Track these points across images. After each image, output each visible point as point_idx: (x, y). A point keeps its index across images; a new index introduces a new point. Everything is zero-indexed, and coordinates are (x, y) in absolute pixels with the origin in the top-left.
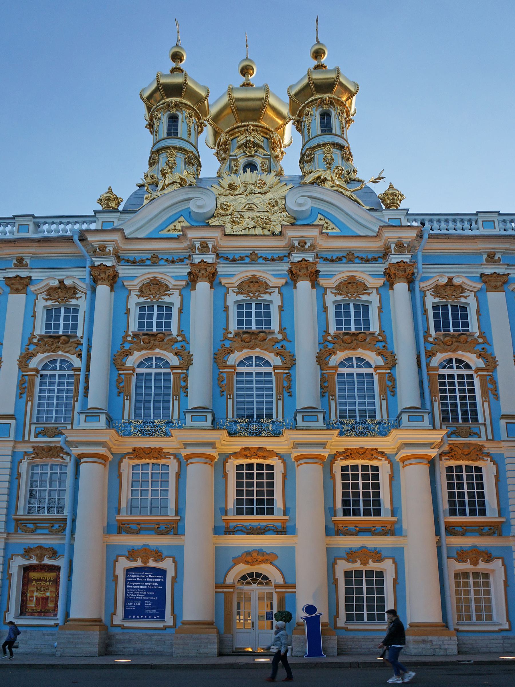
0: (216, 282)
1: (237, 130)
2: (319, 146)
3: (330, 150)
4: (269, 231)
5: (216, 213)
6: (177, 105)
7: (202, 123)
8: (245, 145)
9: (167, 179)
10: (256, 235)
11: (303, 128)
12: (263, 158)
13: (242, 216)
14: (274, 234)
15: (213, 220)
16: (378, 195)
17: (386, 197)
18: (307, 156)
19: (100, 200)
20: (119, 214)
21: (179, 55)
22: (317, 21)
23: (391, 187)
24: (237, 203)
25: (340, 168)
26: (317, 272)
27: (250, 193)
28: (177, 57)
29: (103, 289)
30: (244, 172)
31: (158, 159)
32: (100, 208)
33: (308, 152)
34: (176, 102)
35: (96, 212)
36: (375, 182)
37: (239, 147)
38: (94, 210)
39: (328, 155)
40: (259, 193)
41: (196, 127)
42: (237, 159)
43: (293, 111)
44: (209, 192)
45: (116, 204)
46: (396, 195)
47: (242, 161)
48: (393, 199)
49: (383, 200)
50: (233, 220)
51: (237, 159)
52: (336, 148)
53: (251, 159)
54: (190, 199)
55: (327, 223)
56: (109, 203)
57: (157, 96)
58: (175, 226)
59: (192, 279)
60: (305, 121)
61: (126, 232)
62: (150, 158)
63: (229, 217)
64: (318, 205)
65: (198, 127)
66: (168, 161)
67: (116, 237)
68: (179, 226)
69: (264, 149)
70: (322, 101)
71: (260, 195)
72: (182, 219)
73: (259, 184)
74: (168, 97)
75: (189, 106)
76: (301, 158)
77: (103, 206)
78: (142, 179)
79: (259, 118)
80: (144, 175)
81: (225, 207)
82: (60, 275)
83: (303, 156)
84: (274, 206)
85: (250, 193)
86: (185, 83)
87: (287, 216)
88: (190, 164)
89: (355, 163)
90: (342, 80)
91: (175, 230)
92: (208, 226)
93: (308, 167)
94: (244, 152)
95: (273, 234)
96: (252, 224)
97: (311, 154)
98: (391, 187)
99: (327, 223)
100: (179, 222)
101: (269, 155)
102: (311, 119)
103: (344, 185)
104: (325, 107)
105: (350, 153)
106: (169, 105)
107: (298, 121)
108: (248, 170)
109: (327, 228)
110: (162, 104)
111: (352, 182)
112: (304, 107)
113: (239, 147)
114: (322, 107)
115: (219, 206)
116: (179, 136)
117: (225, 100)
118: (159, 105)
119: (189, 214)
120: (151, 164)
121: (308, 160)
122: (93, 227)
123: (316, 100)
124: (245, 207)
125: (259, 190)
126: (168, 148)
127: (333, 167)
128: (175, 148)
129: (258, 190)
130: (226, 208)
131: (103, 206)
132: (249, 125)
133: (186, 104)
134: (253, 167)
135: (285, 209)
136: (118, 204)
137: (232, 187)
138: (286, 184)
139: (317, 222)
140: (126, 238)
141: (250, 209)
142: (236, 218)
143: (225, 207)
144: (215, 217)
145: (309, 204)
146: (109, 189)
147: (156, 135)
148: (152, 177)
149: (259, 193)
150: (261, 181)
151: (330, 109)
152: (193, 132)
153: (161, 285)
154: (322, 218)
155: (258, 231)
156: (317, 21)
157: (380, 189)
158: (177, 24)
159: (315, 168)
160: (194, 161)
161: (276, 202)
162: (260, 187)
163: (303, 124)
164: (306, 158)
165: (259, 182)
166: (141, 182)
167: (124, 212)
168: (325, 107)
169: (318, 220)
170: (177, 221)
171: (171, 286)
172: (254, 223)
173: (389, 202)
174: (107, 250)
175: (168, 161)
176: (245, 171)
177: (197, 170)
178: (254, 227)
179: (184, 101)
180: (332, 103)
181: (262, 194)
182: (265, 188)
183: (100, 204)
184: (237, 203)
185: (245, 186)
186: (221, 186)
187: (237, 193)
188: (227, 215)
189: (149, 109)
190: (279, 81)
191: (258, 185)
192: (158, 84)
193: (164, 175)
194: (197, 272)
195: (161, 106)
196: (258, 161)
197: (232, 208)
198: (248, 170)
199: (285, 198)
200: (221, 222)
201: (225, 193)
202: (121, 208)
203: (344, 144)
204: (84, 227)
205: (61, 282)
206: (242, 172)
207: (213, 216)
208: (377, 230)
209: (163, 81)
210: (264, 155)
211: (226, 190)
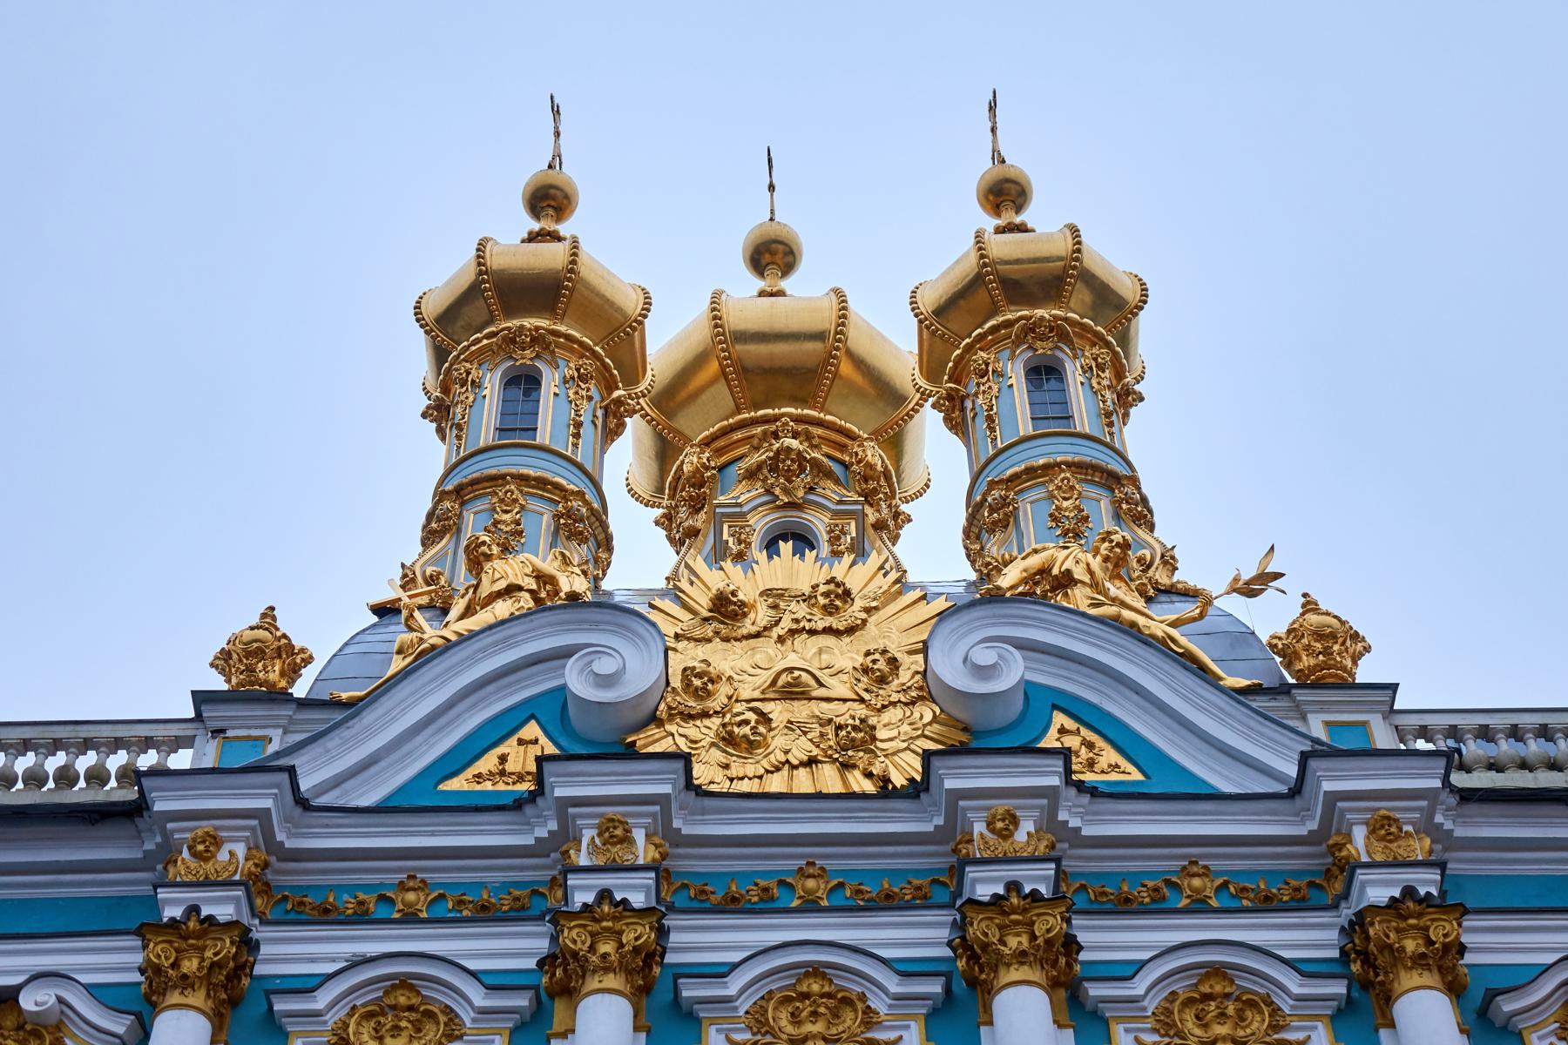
0: (662, 994)
1: (738, 435)
2: (1031, 472)
3: (1072, 488)
4: (869, 775)
5: (662, 706)
6: (539, 340)
7: (619, 402)
8: (774, 465)
9: (485, 579)
10: (819, 796)
11: (970, 415)
12: (836, 514)
13: (764, 718)
14: (886, 790)
15: (653, 731)
16: (1265, 639)
17: (1299, 646)
18: (992, 510)
19: (225, 655)
20: (287, 711)
21: (554, 198)
22: (992, 108)
23: (1310, 606)
24: (743, 667)
25: (1117, 538)
26: (1071, 945)
27: (793, 632)
28: (548, 200)
30: (770, 557)
31: (460, 516)
32: (218, 683)
33: (996, 493)
34: (537, 329)
35: (201, 698)
36: (1250, 589)
37: (751, 475)
38: (194, 693)
39: (1065, 504)
40: (828, 631)
41: (600, 413)
42: (743, 515)
43: (931, 366)
44: (640, 627)
45: (282, 674)
46: (1333, 636)
47: (760, 523)
48: (1327, 652)
49: (1289, 657)
50: (731, 733)
51: (743, 515)
52: (1092, 482)
53: (793, 516)
54: (565, 653)
55: (1090, 746)
56: (256, 671)
57: (476, 311)
58: (503, 759)
59: (562, 979)
60: (976, 395)
61: (305, 785)
62: (430, 516)
63: (716, 722)
64: (1049, 677)
65: (606, 415)
66: (496, 523)
67: (262, 798)
68: (520, 759)
69: (837, 482)
71: (829, 641)
72: (532, 730)
73: (826, 595)
74: (510, 313)
75: (581, 344)
76: (972, 518)
77: (234, 680)
78: (391, 581)
79: (815, 396)
80: (400, 572)
81: (697, 682)
83: (974, 510)
84: (882, 680)
85: (792, 632)
86: (571, 271)
87: (935, 719)
88: (578, 537)
89: (1167, 530)
90: (1088, 261)
91: (502, 773)
92: (630, 753)
93: (994, 548)
94: (768, 492)
95: (884, 787)
96: (801, 748)
97: (1004, 502)
98: (1310, 606)
99: (1090, 746)
100: (521, 742)
101: (856, 502)
102: (995, 388)
103: (1140, 603)
104: (1043, 348)
105: (1144, 500)
106: (511, 341)
107: (950, 397)
108: (786, 547)
109: (1091, 764)
110: (488, 337)
111: (1163, 598)
112: (969, 349)
113: (751, 475)
114: (1030, 347)
115: (676, 682)
116: (543, 437)
117: (701, 335)
118: (479, 340)
119: (556, 709)
120: (430, 537)
121: (995, 523)
122: (181, 760)
123: (1008, 324)
124: (774, 683)
125: (830, 621)
126: (497, 479)
127: (1093, 537)
128: (523, 479)
130: (704, 688)
131: (234, 680)
132: (783, 415)
133: (568, 337)
134: (803, 541)
136: (293, 673)
137: (726, 609)
138: (924, 597)
139: (1050, 741)
140: (302, 802)
142: (739, 724)
143: (700, 683)
144: (660, 723)
145: (1014, 671)
146: (264, 616)
147: (459, 437)
148: (431, 580)
149: (828, 631)
150: (832, 586)
151: (1060, 355)
152: (587, 431)
153: (430, 1015)
154: (1070, 724)
155: (829, 779)
156: (992, 108)
157: (1269, 617)
158: (556, 111)
159: (1021, 549)
160: (587, 528)
161: (893, 662)
162: (829, 610)
163: (968, 404)
164: (988, 517)
165: (822, 589)
166: (388, 592)
167: (303, 704)
168: (1043, 348)
169: (1053, 732)
170: (513, 741)
172: (810, 746)
173: (1312, 662)
174: (223, 856)
175: (496, 523)
176: (771, 547)
177: (596, 560)
178: (811, 762)
179: (562, 328)
180: (1064, 337)
181: (836, 633)
182: (855, 611)
183: (222, 672)
184: (743, 667)
185: (775, 607)
186: (685, 606)
187: (745, 631)
188: (705, 715)
189: (440, 355)
190: (880, 280)
191: (822, 601)
192: (481, 273)
193: (477, 561)
194: (582, 947)
195: (485, 342)
196: (819, 523)
197: (723, 690)
198: (786, 547)
199: (924, 649)
200: (682, 742)
201: (697, 633)
202: (300, 690)
203: (1116, 466)
204: (148, 760)
206: (762, 556)
207: (654, 719)
208: (1293, 771)
209: (496, 261)
210: (840, 502)
211: (706, 619)
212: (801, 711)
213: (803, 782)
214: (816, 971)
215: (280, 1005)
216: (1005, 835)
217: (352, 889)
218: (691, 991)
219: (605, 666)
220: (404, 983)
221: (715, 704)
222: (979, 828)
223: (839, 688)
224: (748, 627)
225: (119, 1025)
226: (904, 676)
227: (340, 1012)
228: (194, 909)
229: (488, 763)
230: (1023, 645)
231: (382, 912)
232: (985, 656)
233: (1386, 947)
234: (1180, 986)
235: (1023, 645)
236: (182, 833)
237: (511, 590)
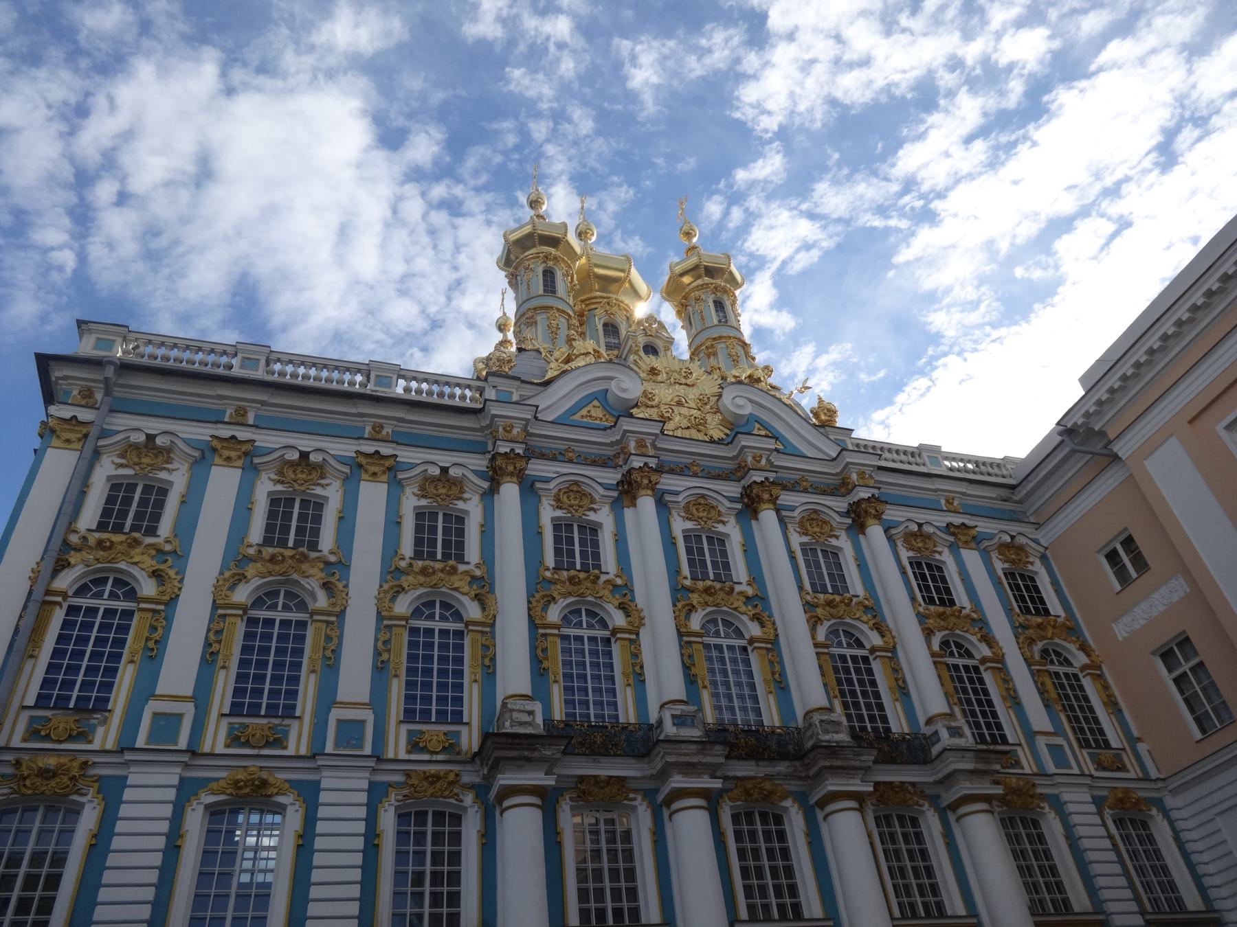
14: (712, 441)
29: (510, 492)
44: (632, 373)
54: (611, 378)
63: (655, 410)
70: (716, 288)
82: (445, 459)
96: (685, 423)
128: (558, 310)
129: (683, 381)
135: (718, 411)
141: (679, 404)
171: (597, 497)
205: (445, 470)
207: (636, 405)
212: (684, 411)
213: (687, 434)
214: (703, 496)
215: (538, 485)
216: (759, 462)
217: (551, 449)
218: (668, 498)
219: (624, 386)
220: (576, 483)
221: (654, 403)
222: (750, 459)
223: (692, 405)
224: (659, 378)
225: (486, 485)
226: (711, 403)
227: (555, 491)
228: (512, 450)
229: (584, 412)
230: (751, 401)
231: (561, 458)
232: (740, 401)
233: (866, 512)
234: (805, 514)
235: (751, 401)
236: (499, 421)
237: (587, 354)
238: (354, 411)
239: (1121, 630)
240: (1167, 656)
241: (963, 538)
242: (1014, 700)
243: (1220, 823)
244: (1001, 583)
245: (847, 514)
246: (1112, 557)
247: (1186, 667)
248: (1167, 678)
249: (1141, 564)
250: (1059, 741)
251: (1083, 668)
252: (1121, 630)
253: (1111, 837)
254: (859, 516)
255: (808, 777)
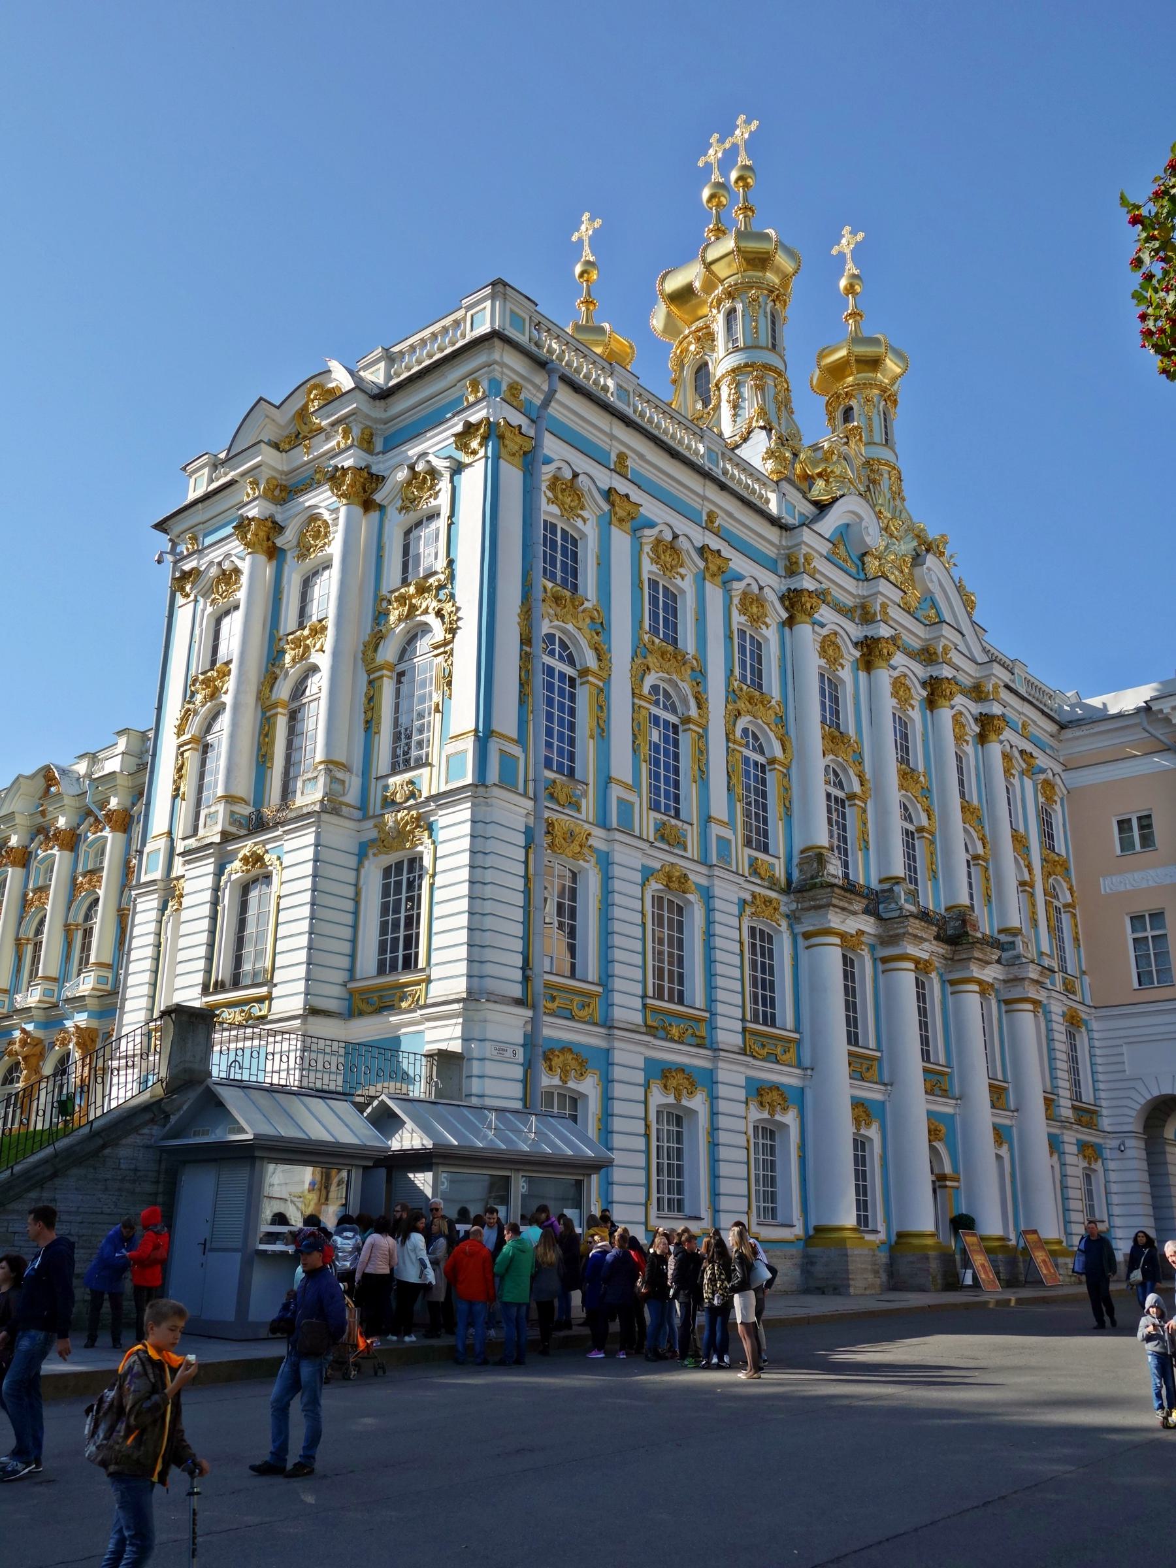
225: (785, 615)
238: (700, 490)
239: (1107, 885)
240: (1137, 920)
241: (621, 513)
242: (602, 732)
243: (1125, 1049)
244: (731, 639)
245: (924, 684)
246: (1124, 825)
247: (1149, 933)
248: (1130, 937)
249: (1147, 840)
250: (632, 797)
251: (1066, 906)
252: (1107, 885)
253: (741, 943)
254: (870, 654)
255: (952, 959)
